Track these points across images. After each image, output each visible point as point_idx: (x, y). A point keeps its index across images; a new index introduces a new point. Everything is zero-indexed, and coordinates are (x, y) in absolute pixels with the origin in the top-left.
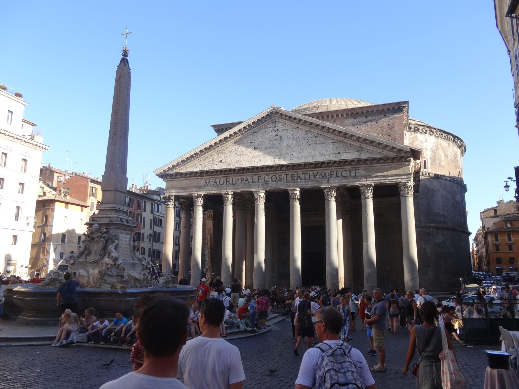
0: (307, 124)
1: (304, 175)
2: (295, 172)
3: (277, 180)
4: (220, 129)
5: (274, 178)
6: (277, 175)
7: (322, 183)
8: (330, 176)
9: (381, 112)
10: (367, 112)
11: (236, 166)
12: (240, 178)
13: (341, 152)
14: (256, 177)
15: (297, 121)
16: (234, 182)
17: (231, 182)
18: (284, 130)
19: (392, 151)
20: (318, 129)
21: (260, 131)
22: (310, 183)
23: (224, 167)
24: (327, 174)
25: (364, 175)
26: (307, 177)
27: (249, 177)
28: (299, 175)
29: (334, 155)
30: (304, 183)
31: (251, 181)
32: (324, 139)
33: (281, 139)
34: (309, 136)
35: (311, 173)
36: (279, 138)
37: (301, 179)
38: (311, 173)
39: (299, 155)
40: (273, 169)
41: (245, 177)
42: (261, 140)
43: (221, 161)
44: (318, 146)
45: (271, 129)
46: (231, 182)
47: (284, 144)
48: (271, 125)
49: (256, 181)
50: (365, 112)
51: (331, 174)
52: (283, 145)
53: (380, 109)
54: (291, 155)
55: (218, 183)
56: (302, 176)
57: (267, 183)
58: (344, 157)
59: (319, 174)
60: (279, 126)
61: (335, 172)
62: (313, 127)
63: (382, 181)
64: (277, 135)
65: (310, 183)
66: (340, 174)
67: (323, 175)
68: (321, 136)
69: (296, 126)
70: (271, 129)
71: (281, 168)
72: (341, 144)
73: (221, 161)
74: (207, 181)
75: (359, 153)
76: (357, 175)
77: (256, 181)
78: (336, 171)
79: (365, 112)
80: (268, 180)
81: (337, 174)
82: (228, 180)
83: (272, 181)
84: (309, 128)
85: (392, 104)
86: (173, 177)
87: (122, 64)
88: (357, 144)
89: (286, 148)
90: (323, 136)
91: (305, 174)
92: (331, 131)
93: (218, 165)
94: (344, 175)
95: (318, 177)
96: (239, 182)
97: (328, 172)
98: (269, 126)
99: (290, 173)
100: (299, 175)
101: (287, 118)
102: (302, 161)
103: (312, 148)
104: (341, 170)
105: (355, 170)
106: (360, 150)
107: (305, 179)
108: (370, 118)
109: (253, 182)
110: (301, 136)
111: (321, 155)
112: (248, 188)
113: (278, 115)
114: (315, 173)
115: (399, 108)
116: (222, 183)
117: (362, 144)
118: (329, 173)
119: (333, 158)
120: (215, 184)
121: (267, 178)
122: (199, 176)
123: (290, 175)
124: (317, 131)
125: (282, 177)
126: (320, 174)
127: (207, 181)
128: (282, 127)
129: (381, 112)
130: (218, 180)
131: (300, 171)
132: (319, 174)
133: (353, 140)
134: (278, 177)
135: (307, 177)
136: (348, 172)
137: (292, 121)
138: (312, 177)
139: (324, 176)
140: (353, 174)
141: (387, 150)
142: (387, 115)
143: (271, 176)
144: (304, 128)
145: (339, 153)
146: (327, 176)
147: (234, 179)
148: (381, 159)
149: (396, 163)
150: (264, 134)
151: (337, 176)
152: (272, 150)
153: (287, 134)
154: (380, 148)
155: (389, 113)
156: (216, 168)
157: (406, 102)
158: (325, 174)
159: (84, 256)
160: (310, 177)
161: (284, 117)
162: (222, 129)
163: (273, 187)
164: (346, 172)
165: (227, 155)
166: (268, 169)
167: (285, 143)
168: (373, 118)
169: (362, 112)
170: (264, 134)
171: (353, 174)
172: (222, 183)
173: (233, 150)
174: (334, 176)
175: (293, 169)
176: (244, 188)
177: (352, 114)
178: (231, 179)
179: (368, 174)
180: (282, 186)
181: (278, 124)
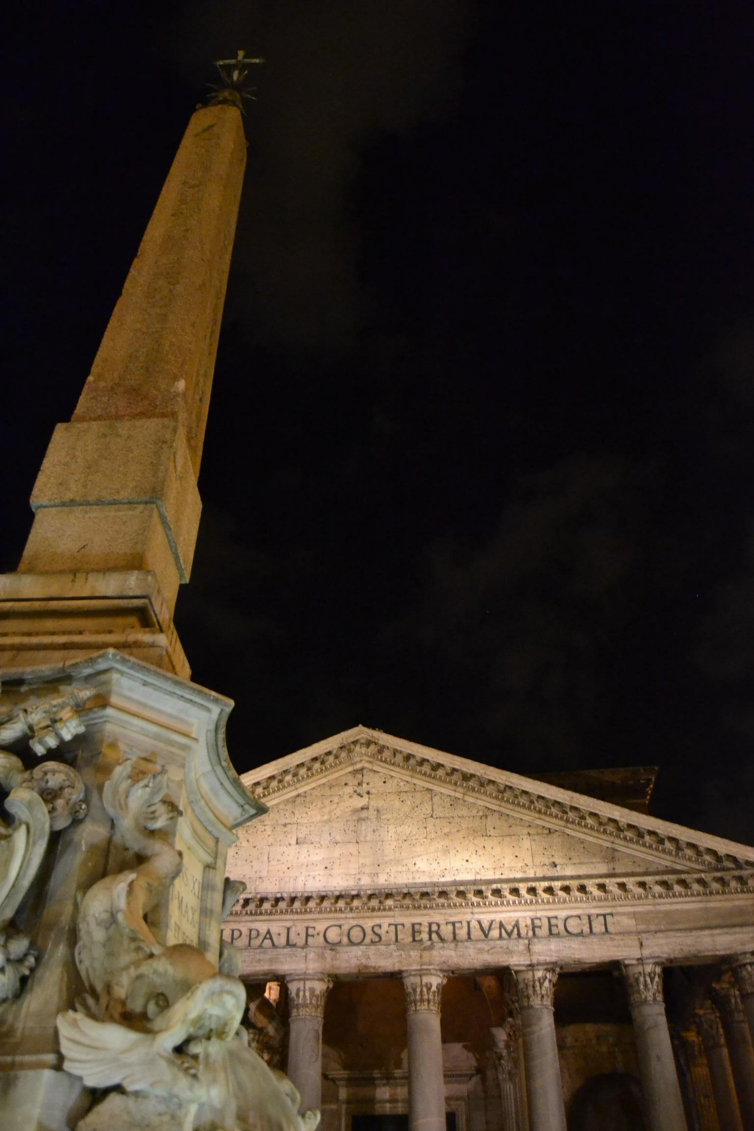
1: (450, 927)
3: (367, 940)
6: (368, 924)
8: (531, 933)
12: (245, 931)
13: (557, 861)
15: (426, 768)
21: (315, 793)
24: (522, 925)
25: (634, 929)
26: (462, 933)
28: (434, 928)
30: (453, 953)
31: (283, 940)
34: (461, 813)
35: (474, 924)
37: (442, 940)
38: (474, 924)
39: (435, 865)
40: (356, 903)
44: (489, 843)
49: (300, 941)
54: (411, 866)
56: (447, 931)
57: (333, 946)
60: (374, 783)
61: (545, 922)
63: (686, 949)
68: (496, 815)
69: (421, 783)
70: (349, 790)
72: (556, 839)
76: (611, 929)
77: (300, 941)
78: (549, 919)
84: (460, 789)
88: (605, 842)
89: (395, 844)
90: (501, 814)
91: (454, 924)
95: (495, 933)
99: (407, 919)
103: (472, 848)
104: (563, 914)
105: (604, 916)
106: (611, 856)
109: (288, 943)
117: (617, 841)
118: (529, 922)
121: (333, 935)
123: (408, 926)
124: (483, 802)
125: (382, 932)
132: (496, 925)
134: (369, 931)
135: (462, 933)
136: (585, 921)
137: (413, 770)
138: (476, 933)
140: (598, 927)
143: (346, 928)
144: (446, 790)
146: (523, 932)
149: (718, 897)
150: (327, 802)
153: (397, 804)
158: (517, 925)
160: (469, 933)
163: (354, 962)
164: (577, 920)
166: (341, 904)
170: (327, 802)
171: (598, 927)
179: (642, 927)
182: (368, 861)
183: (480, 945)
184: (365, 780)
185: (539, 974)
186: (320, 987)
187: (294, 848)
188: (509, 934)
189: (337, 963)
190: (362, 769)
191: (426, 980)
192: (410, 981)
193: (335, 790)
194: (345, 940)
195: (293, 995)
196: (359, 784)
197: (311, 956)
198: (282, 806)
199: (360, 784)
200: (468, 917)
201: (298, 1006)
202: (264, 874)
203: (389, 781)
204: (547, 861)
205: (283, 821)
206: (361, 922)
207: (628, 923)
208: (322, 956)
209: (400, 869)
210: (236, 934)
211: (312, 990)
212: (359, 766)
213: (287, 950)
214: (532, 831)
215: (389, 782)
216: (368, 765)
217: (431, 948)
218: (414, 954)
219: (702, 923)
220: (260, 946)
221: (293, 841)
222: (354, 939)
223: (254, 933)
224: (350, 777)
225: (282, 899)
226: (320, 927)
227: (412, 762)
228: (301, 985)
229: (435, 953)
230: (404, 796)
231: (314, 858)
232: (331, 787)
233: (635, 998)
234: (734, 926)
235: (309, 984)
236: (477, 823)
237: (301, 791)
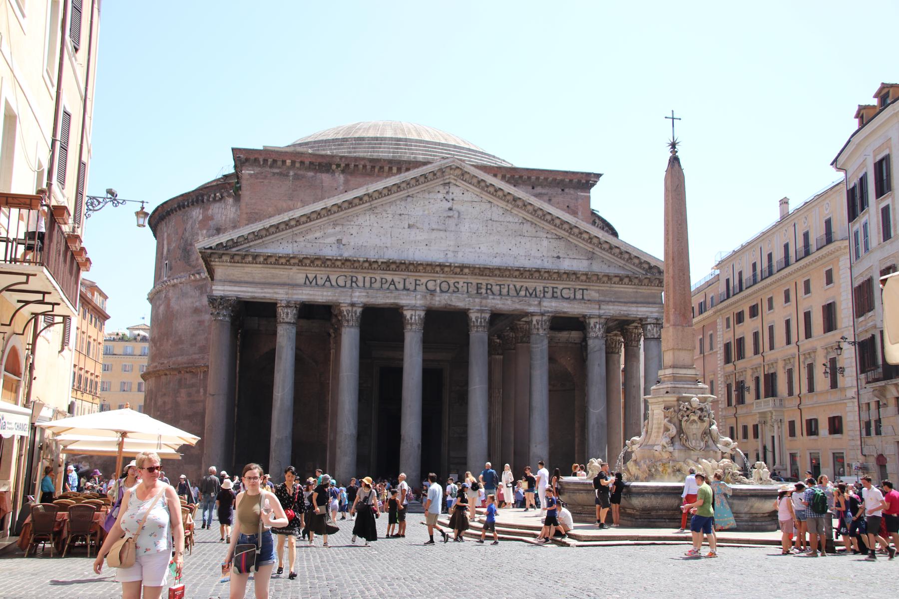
0: (508, 197)
1: (498, 287)
2: (483, 281)
3: (451, 290)
4: (252, 158)
5: (444, 286)
6: (451, 281)
7: (530, 305)
9: (558, 184)
10: (538, 178)
11: (372, 256)
12: (378, 279)
14: (412, 280)
15: (491, 189)
16: (367, 284)
17: (361, 284)
18: (463, 202)
19: (640, 268)
20: (528, 212)
21: (419, 195)
22: (509, 302)
23: (346, 255)
24: (538, 290)
26: (505, 291)
27: (396, 279)
29: (550, 260)
30: (499, 302)
31: (401, 286)
32: (534, 230)
33: (459, 216)
35: (511, 286)
36: (456, 215)
37: (493, 294)
39: (491, 250)
40: (446, 269)
41: (389, 278)
42: (421, 213)
43: (339, 241)
44: (523, 240)
45: (440, 196)
46: (361, 284)
47: (465, 227)
48: (441, 189)
49: (412, 287)
50: (533, 178)
51: (544, 292)
52: (463, 229)
53: (559, 178)
55: (334, 283)
56: (496, 289)
58: (566, 265)
59: (524, 288)
60: (456, 192)
61: (551, 289)
62: (518, 206)
64: (450, 209)
65: (509, 302)
66: (559, 293)
67: (531, 291)
68: (529, 224)
69: (486, 197)
70: (440, 196)
71: (462, 270)
72: (562, 244)
73: (339, 241)
74: (311, 276)
75: (590, 261)
76: (585, 297)
77: (412, 287)
79: (533, 178)
80: (433, 288)
81: (553, 292)
82: (354, 279)
83: (442, 291)
84: (510, 205)
85: (577, 173)
86: (237, 258)
87: (676, 165)
88: (589, 247)
91: (500, 285)
92: (549, 217)
93: (335, 247)
94: (565, 296)
95: (523, 293)
96: (377, 285)
97: (540, 288)
98: (437, 189)
99: (474, 280)
100: (489, 287)
101: (475, 181)
102: (496, 262)
103: (513, 242)
104: (561, 287)
105: (583, 290)
106: (591, 257)
107: (500, 294)
108: (539, 190)
109: (405, 289)
110: (495, 217)
111: (528, 256)
112: (395, 298)
113: (458, 172)
114: (518, 287)
115: (587, 182)
116: (341, 283)
118: (542, 289)
119: (548, 264)
120: (328, 284)
121: (431, 285)
122: (294, 265)
123: (474, 284)
124: (523, 214)
126: (527, 289)
127: (311, 276)
128: (464, 197)
129: (558, 184)
130: (333, 278)
131: (492, 281)
132: (524, 288)
133: (584, 239)
134: (452, 285)
135: (505, 291)
136: (572, 291)
137: (483, 189)
138: (513, 292)
139: (533, 294)
140: (579, 296)
141: (634, 264)
142: (566, 190)
143: (438, 282)
144: (502, 204)
145: (558, 257)
147: (368, 279)
148: (627, 276)
151: (553, 297)
152: (442, 234)
154: (624, 259)
155: (570, 188)
156: (330, 252)
157: (598, 176)
158: (535, 289)
159: (677, 439)
161: (467, 177)
162: (256, 160)
163: (443, 302)
164: (568, 291)
165: (354, 231)
167: (467, 226)
168: (544, 191)
169: (529, 178)
170: (426, 203)
171: (579, 296)
172: (341, 283)
173: (366, 224)
174: (549, 295)
175: (482, 275)
176: (388, 297)
177: (513, 177)
178: (360, 278)
179: (602, 298)
180: (459, 302)
181: (453, 189)
182: (452, 243)
183: (514, 299)
184: (451, 190)
185: (544, 318)
186: (422, 314)
187: (407, 231)
188: (531, 295)
189: (433, 302)
190: (449, 183)
191: (483, 315)
192: (473, 316)
193: (432, 195)
194: (438, 289)
195: (408, 317)
196: (447, 193)
197: (419, 297)
198: (398, 202)
199: (447, 193)
200: (508, 283)
201: (411, 324)
202: (389, 245)
203: (466, 193)
204: (556, 255)
205: (400, 212)
206: (447, 280)
207: (595, 295)
208: (424, 297)
209: (471, 250)
210: (373, 280)
211: (419, 316)
212: (447, 181)
213: (405, 292)
214: (549, 236)
215: (466, 193)
216: (453, 181)
217: (486, 298)
218: (477, 300)
219: (633, 300)
220: (388, 289)
221: (406, 226)
222: (443, 289)
223: (384, 281)
224: (442, 187)
225: (405, 263)
226: (424, 280)
227: (483, 184)
228: (413, 313)
229: (489, 301)
230: (475, 204)
231: (419, 238)
232: (429, 193)
233: (592, 334)
234: (649, 303)
235: (418, 312)
236: (517, 227)
237: (410, 194)
